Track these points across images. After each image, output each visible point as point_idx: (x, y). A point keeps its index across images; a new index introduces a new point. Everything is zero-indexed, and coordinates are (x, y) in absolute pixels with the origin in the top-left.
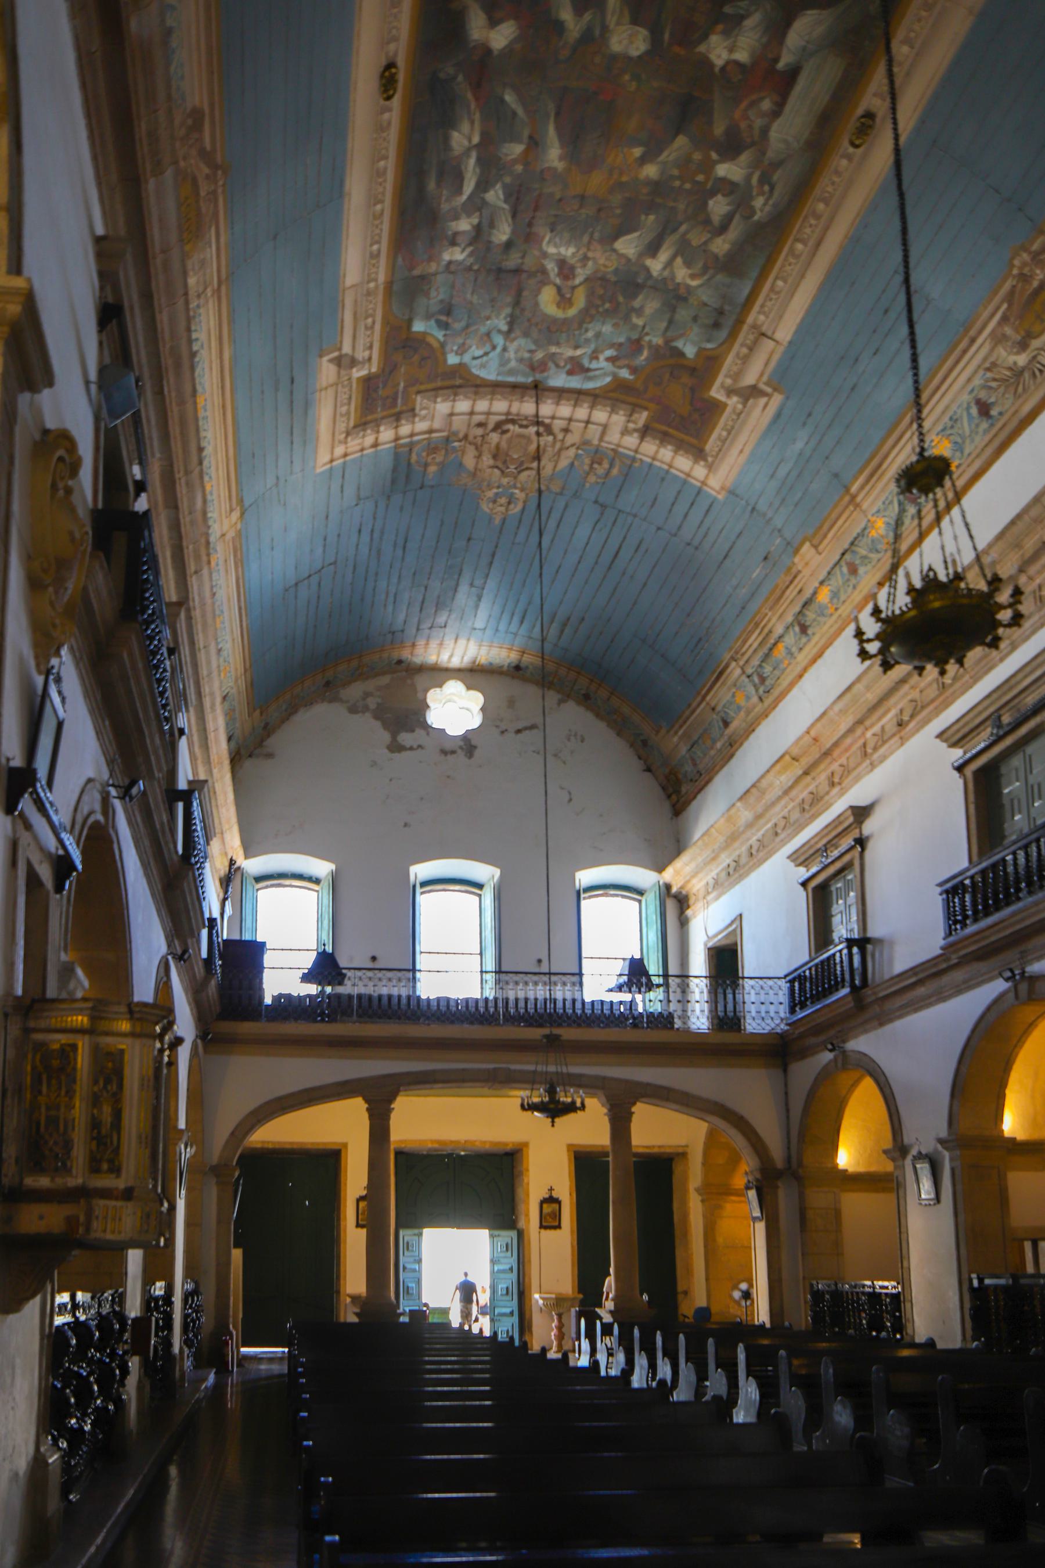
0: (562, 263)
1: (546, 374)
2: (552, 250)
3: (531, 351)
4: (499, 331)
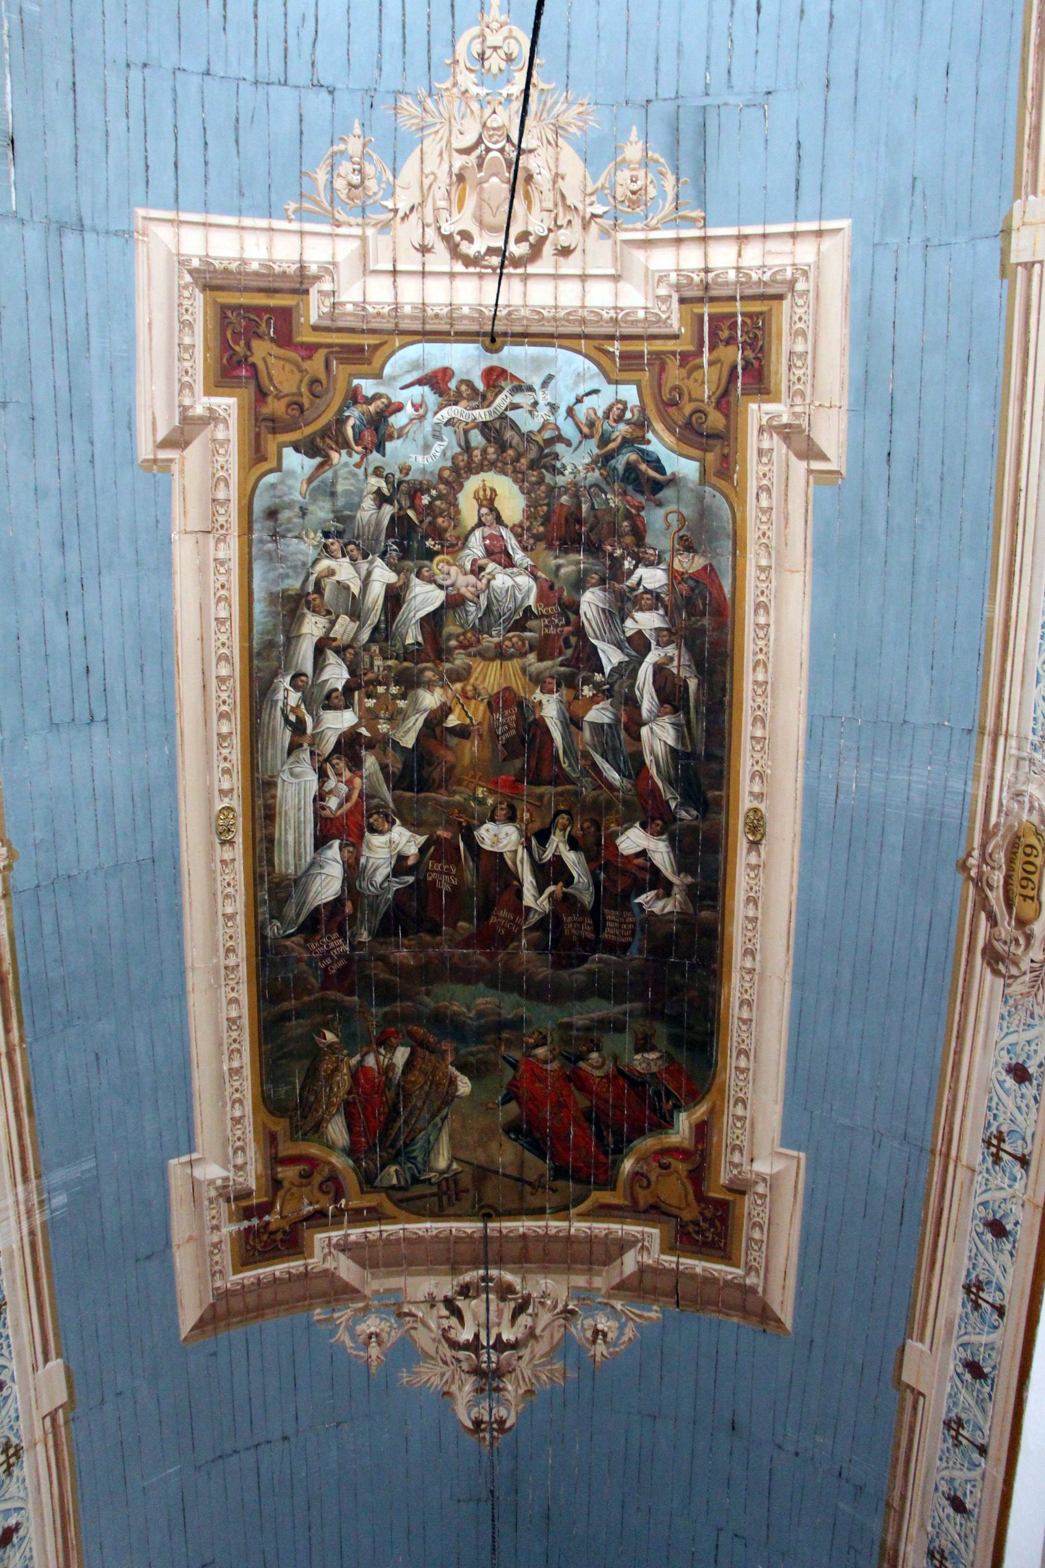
0: (508, 562)
1: (485, 365)
2: (525, 581)
3: (515, 407)
4: (569, 444)
